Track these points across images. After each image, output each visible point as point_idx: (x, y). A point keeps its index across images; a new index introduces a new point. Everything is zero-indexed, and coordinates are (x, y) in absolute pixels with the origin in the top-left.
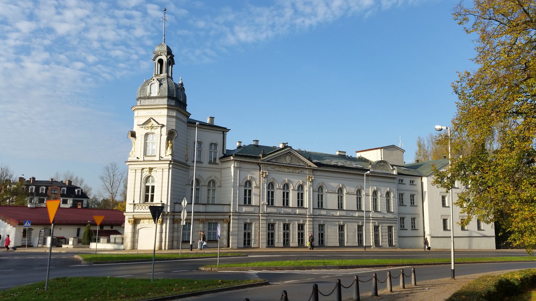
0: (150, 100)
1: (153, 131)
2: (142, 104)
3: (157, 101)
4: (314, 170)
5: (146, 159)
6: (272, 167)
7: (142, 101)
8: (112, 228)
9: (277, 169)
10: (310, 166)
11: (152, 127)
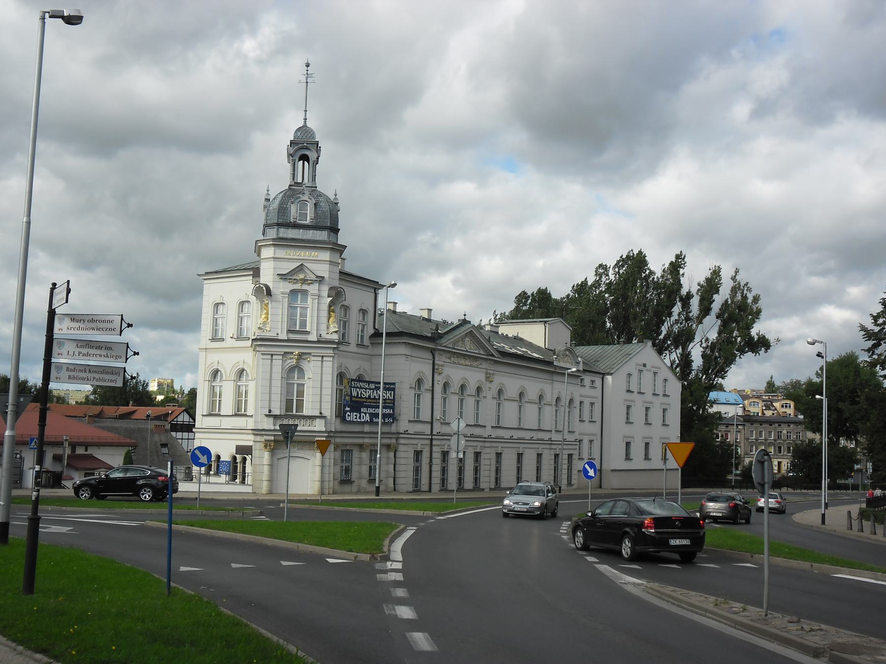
0: (296, 231)
1: (305, 287)
2: (281, 235)
3: (310, 235)
4: (496, 362)
5: (292, 336)
6: (448, 355)
7: (282, 230)
8: (86, 450)
9: (452, 359)
10: (492, 355)
11: (304, 281)
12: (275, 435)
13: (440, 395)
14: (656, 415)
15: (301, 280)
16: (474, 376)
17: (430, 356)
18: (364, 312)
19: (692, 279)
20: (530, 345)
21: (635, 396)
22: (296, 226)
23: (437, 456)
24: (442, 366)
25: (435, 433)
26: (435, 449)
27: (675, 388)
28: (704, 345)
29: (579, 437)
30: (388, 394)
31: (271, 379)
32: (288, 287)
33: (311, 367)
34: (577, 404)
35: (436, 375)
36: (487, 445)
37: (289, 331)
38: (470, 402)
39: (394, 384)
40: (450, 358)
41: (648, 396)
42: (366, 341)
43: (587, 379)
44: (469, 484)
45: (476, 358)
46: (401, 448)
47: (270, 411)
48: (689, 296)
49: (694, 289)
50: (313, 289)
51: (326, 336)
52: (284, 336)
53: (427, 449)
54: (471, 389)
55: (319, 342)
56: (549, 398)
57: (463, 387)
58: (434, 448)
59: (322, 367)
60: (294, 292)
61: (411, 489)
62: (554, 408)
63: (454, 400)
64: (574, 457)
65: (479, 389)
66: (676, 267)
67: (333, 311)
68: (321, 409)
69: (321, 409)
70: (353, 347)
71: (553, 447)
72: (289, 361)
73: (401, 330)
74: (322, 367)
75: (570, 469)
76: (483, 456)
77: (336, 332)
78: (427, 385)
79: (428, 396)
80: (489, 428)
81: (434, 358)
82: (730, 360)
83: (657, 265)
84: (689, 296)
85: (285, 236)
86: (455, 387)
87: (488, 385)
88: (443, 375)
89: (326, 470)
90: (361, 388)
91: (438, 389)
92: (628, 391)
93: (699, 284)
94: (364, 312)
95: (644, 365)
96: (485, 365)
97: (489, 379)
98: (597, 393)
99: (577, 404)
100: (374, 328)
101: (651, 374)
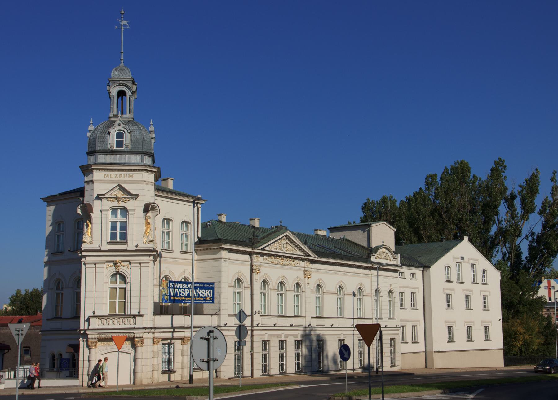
0: (113, 156)
3: (127, 159)
9: (270, 260)
10: (309, 256)
13: (259, 292)
14: (477, 302)
15: (119, 198)
16: (292, 273)
18: (186, 223)
19: (513, 182)
21: (454, 285)
22: (113, 152)
24: (260, 266)
25: (255, 324)
26: (255, 338)
27: (495, 277)
29: (403, 324)
30: (208, 293)
32: (107, 204)
34: (397, 294)
35: (254, 274)
38: (290, 297)
39: (213, 283)
42: (191, 248)
43: (407, 271)
47: (94, 313)
48: (513, 197)
49: (517, 190)
50: (130, 205)
51: (141, 246)
52: (106, 247)
54: (290, 284)
56: (369, 289)
58: (255, 338)
61: (233, 376)
62: (374, 299)
64: (396, 341)
65: (298, 285)
66: (497, 171)
70: (177, 253)
72: (109, 269)
73: (220, 237)
75: (393, 353)
78: (247, 282)
81: (252, 260)
83: (480, 171)
84: (513, 197)
85: (104, 161)
87: (307, 281)
90: (179, 288)
91: (257, 286)
93: (520, 186)
95: (462, 258)
96: (302, 264)
97: (306, 275)
99: (397, 294)
100: (198, 237)
101: (470, 266)
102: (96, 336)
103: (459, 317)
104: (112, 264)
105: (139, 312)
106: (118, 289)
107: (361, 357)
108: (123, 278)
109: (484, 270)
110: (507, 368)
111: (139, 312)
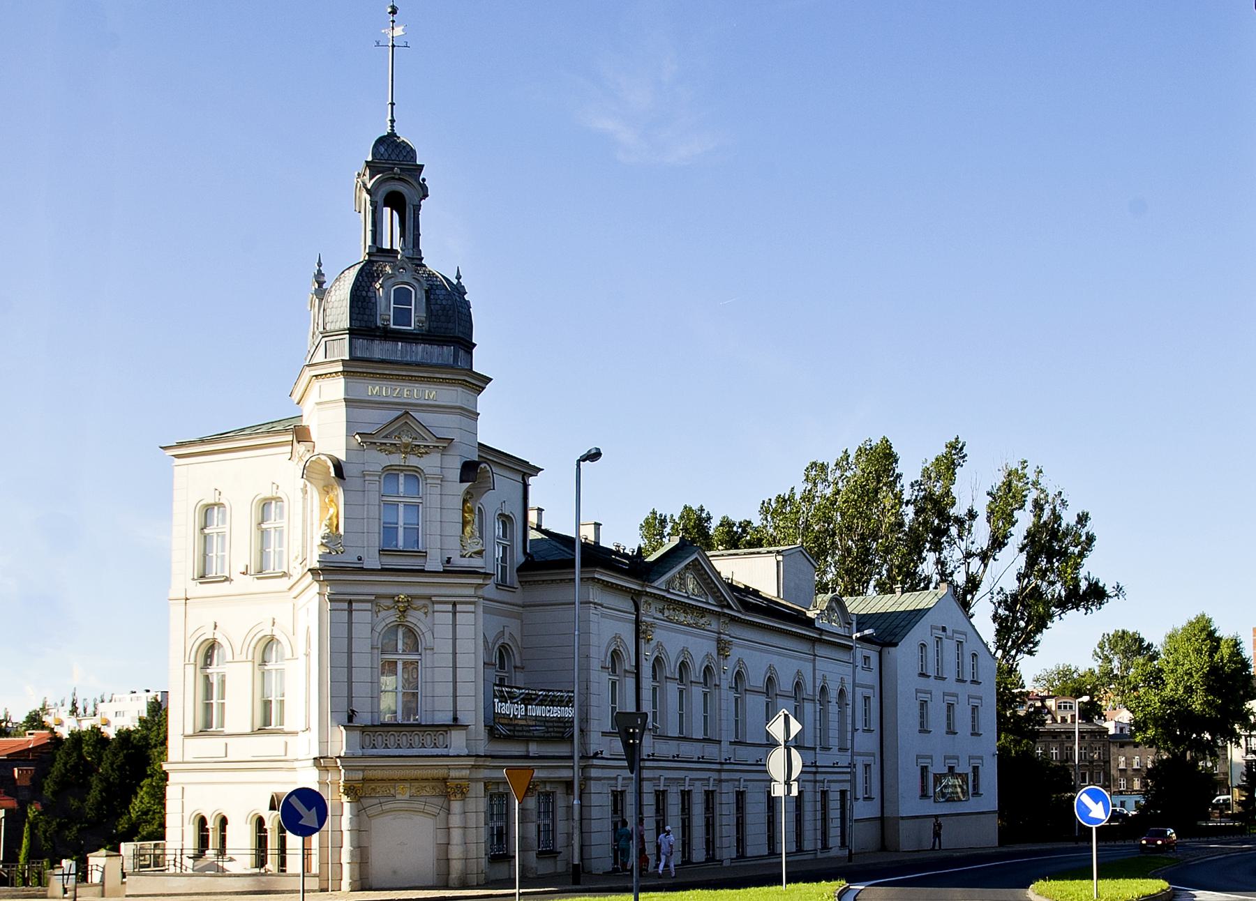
0: (388, 345)
1: (413, 461)
3: (419, 351)
4: (733, 619)
10: (730, 607)
12: (364, 768)
15: (406, 445)
17: (628, 605)
20: (756, 593)
21: (931, 684)
22: (388, 335)
23: (649, 799)
24: (652, 625)
28: (997, 598)
31: (350, 653)
32: (379, 460)
33: (435, 627)
35: (642, 642)
36: (724, 776)
37: (383, 552)
40: (662, 611)
41: (951, 685)
42: (512, 577)
44: (699, 855)
45: (703, 612)
46: (594, 787)
50: (429, 463)
52: (373, 562)
53: (631, 790)
54: (696, 672)
55: (445, 572)
57: (683, 666)
58: (645, 784)
59: (454, 625)
60: (391, 472)
63: (672, 689)
66: (950, 461)
67: (471, 511)
68: (455, 711)
69: (455, 711)
71: (819, 777)
74: (454, 625)
76: (717, 796)
77: (479, 553)
78: (629, 663)
79: (630, 682)
80: (725, 745)
81: (637, 609)
82: (1041, 623)
85: (367, 355)
86: (671, 669)
88: (653, 643)
89: (472, 834)
92: (922, 675)
94: (506, 520)
95: (944, 629)
97: (723, 648)
98: (871, 678)
102: (359, 775)
103: (938, 749)
104: (389, 603)
105: (455, 719)
106: (400, 666)
107: (708, 833)
108: (411, 633)
109: (974, 655)
110: (1004, 850)
111: (455, 719)
